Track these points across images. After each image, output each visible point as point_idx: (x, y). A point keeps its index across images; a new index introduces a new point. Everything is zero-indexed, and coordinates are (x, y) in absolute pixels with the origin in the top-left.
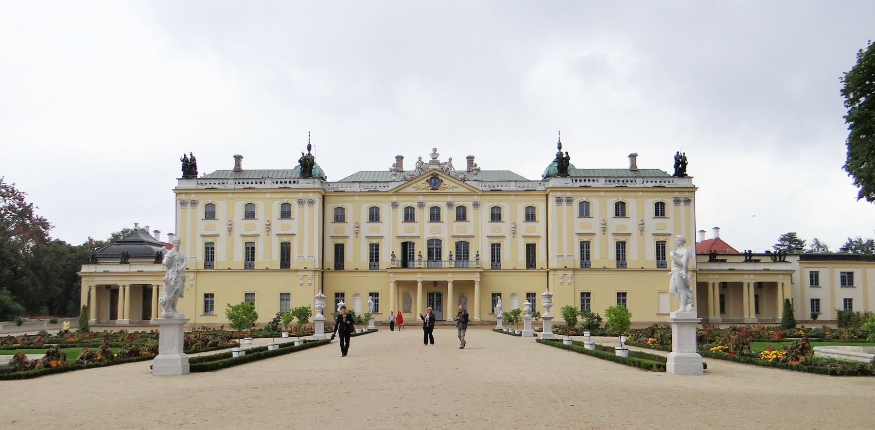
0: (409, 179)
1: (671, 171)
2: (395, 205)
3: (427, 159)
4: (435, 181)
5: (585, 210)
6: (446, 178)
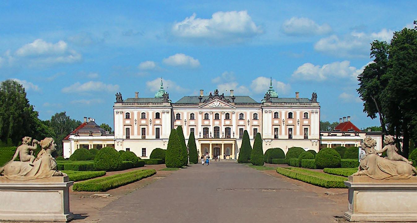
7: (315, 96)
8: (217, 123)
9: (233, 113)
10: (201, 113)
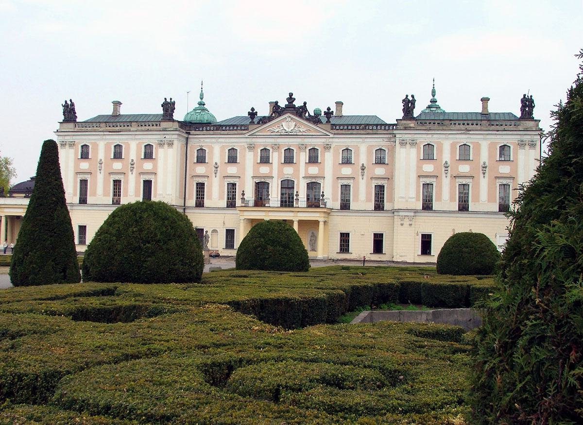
0: (264, 120)
1: (518, 114)
3: (283, 103)
8: (288, 171)
9: (327, 147)
10: (251, 147)
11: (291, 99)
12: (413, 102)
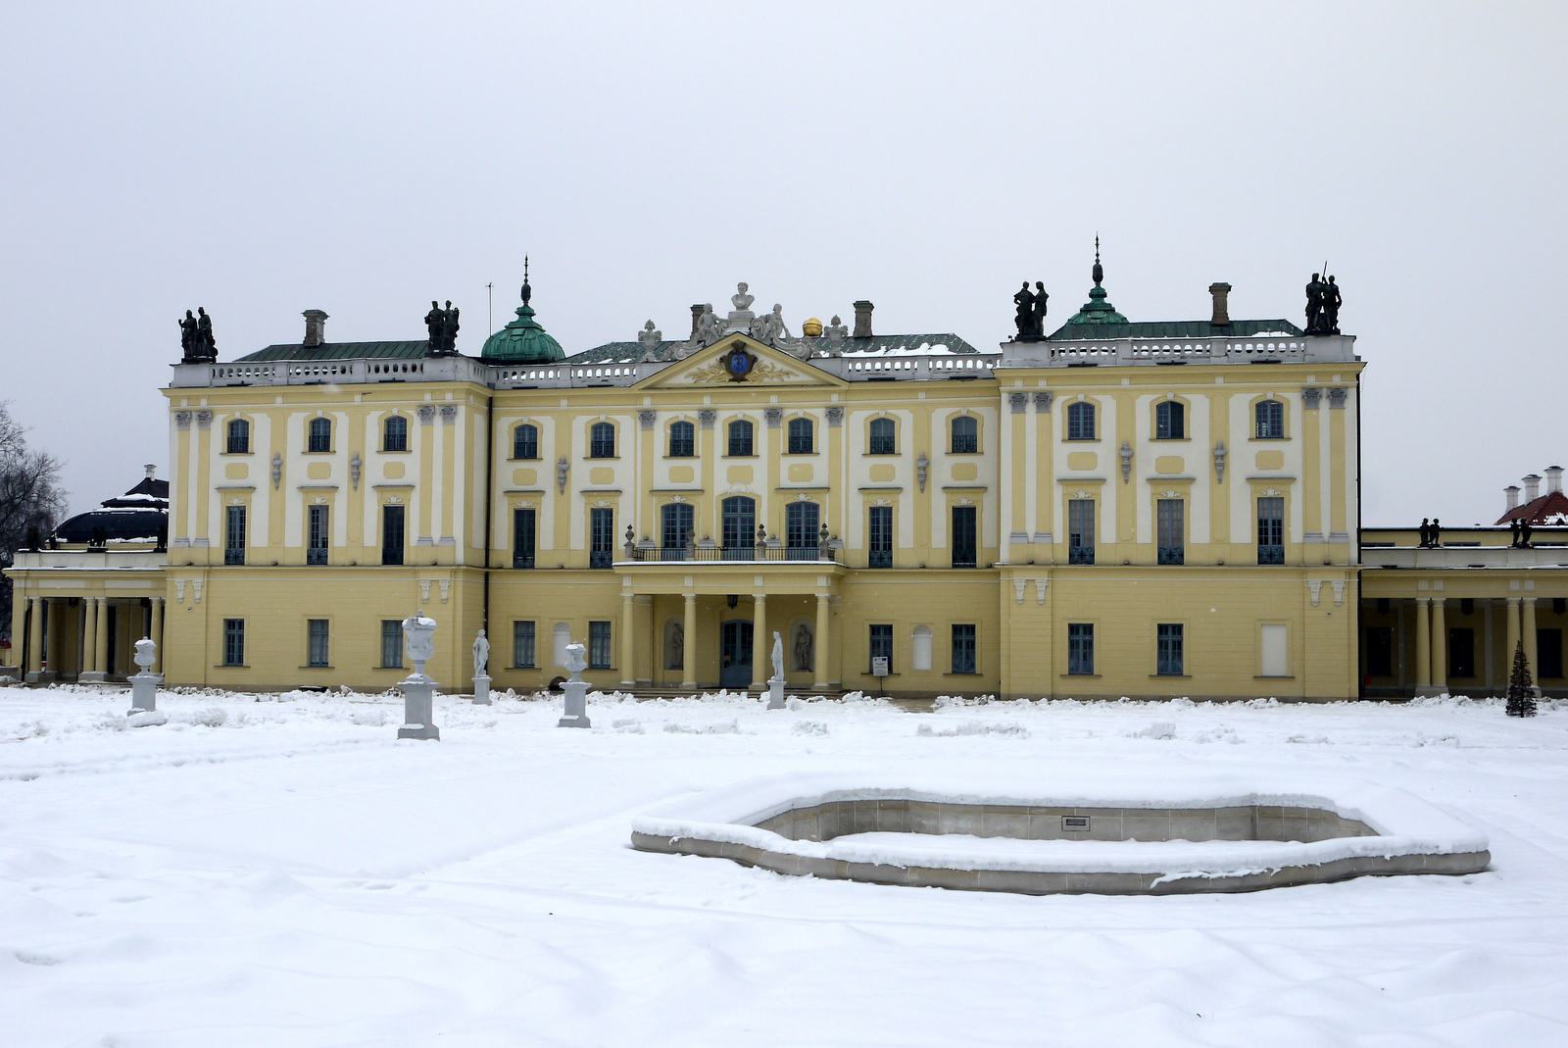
2: (647, 418)
4: (739, 364)
5: (1082, 424)
6: (762, 352)
7: (1323, 298)
11: (743, 298)
12: (1043, 297)
